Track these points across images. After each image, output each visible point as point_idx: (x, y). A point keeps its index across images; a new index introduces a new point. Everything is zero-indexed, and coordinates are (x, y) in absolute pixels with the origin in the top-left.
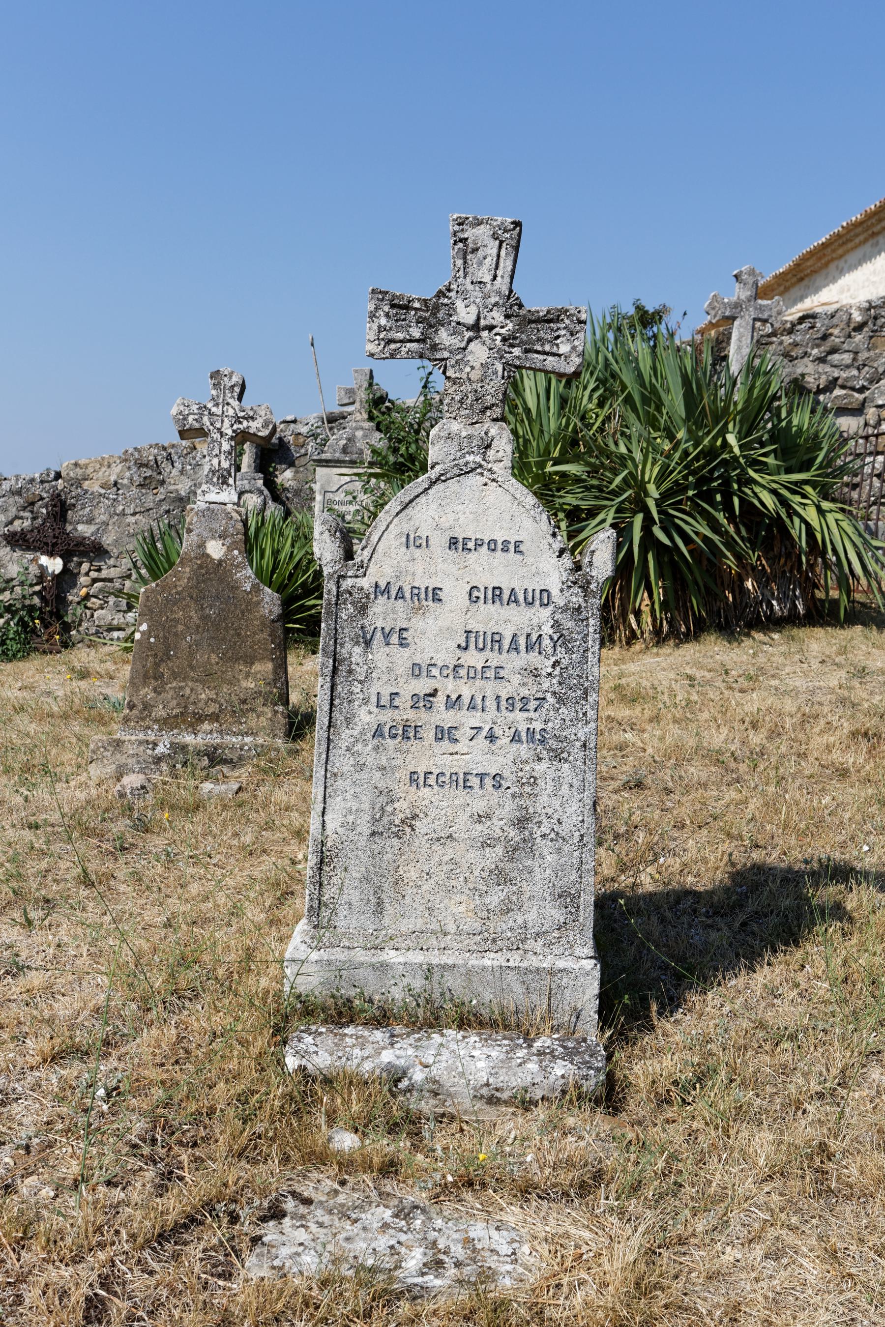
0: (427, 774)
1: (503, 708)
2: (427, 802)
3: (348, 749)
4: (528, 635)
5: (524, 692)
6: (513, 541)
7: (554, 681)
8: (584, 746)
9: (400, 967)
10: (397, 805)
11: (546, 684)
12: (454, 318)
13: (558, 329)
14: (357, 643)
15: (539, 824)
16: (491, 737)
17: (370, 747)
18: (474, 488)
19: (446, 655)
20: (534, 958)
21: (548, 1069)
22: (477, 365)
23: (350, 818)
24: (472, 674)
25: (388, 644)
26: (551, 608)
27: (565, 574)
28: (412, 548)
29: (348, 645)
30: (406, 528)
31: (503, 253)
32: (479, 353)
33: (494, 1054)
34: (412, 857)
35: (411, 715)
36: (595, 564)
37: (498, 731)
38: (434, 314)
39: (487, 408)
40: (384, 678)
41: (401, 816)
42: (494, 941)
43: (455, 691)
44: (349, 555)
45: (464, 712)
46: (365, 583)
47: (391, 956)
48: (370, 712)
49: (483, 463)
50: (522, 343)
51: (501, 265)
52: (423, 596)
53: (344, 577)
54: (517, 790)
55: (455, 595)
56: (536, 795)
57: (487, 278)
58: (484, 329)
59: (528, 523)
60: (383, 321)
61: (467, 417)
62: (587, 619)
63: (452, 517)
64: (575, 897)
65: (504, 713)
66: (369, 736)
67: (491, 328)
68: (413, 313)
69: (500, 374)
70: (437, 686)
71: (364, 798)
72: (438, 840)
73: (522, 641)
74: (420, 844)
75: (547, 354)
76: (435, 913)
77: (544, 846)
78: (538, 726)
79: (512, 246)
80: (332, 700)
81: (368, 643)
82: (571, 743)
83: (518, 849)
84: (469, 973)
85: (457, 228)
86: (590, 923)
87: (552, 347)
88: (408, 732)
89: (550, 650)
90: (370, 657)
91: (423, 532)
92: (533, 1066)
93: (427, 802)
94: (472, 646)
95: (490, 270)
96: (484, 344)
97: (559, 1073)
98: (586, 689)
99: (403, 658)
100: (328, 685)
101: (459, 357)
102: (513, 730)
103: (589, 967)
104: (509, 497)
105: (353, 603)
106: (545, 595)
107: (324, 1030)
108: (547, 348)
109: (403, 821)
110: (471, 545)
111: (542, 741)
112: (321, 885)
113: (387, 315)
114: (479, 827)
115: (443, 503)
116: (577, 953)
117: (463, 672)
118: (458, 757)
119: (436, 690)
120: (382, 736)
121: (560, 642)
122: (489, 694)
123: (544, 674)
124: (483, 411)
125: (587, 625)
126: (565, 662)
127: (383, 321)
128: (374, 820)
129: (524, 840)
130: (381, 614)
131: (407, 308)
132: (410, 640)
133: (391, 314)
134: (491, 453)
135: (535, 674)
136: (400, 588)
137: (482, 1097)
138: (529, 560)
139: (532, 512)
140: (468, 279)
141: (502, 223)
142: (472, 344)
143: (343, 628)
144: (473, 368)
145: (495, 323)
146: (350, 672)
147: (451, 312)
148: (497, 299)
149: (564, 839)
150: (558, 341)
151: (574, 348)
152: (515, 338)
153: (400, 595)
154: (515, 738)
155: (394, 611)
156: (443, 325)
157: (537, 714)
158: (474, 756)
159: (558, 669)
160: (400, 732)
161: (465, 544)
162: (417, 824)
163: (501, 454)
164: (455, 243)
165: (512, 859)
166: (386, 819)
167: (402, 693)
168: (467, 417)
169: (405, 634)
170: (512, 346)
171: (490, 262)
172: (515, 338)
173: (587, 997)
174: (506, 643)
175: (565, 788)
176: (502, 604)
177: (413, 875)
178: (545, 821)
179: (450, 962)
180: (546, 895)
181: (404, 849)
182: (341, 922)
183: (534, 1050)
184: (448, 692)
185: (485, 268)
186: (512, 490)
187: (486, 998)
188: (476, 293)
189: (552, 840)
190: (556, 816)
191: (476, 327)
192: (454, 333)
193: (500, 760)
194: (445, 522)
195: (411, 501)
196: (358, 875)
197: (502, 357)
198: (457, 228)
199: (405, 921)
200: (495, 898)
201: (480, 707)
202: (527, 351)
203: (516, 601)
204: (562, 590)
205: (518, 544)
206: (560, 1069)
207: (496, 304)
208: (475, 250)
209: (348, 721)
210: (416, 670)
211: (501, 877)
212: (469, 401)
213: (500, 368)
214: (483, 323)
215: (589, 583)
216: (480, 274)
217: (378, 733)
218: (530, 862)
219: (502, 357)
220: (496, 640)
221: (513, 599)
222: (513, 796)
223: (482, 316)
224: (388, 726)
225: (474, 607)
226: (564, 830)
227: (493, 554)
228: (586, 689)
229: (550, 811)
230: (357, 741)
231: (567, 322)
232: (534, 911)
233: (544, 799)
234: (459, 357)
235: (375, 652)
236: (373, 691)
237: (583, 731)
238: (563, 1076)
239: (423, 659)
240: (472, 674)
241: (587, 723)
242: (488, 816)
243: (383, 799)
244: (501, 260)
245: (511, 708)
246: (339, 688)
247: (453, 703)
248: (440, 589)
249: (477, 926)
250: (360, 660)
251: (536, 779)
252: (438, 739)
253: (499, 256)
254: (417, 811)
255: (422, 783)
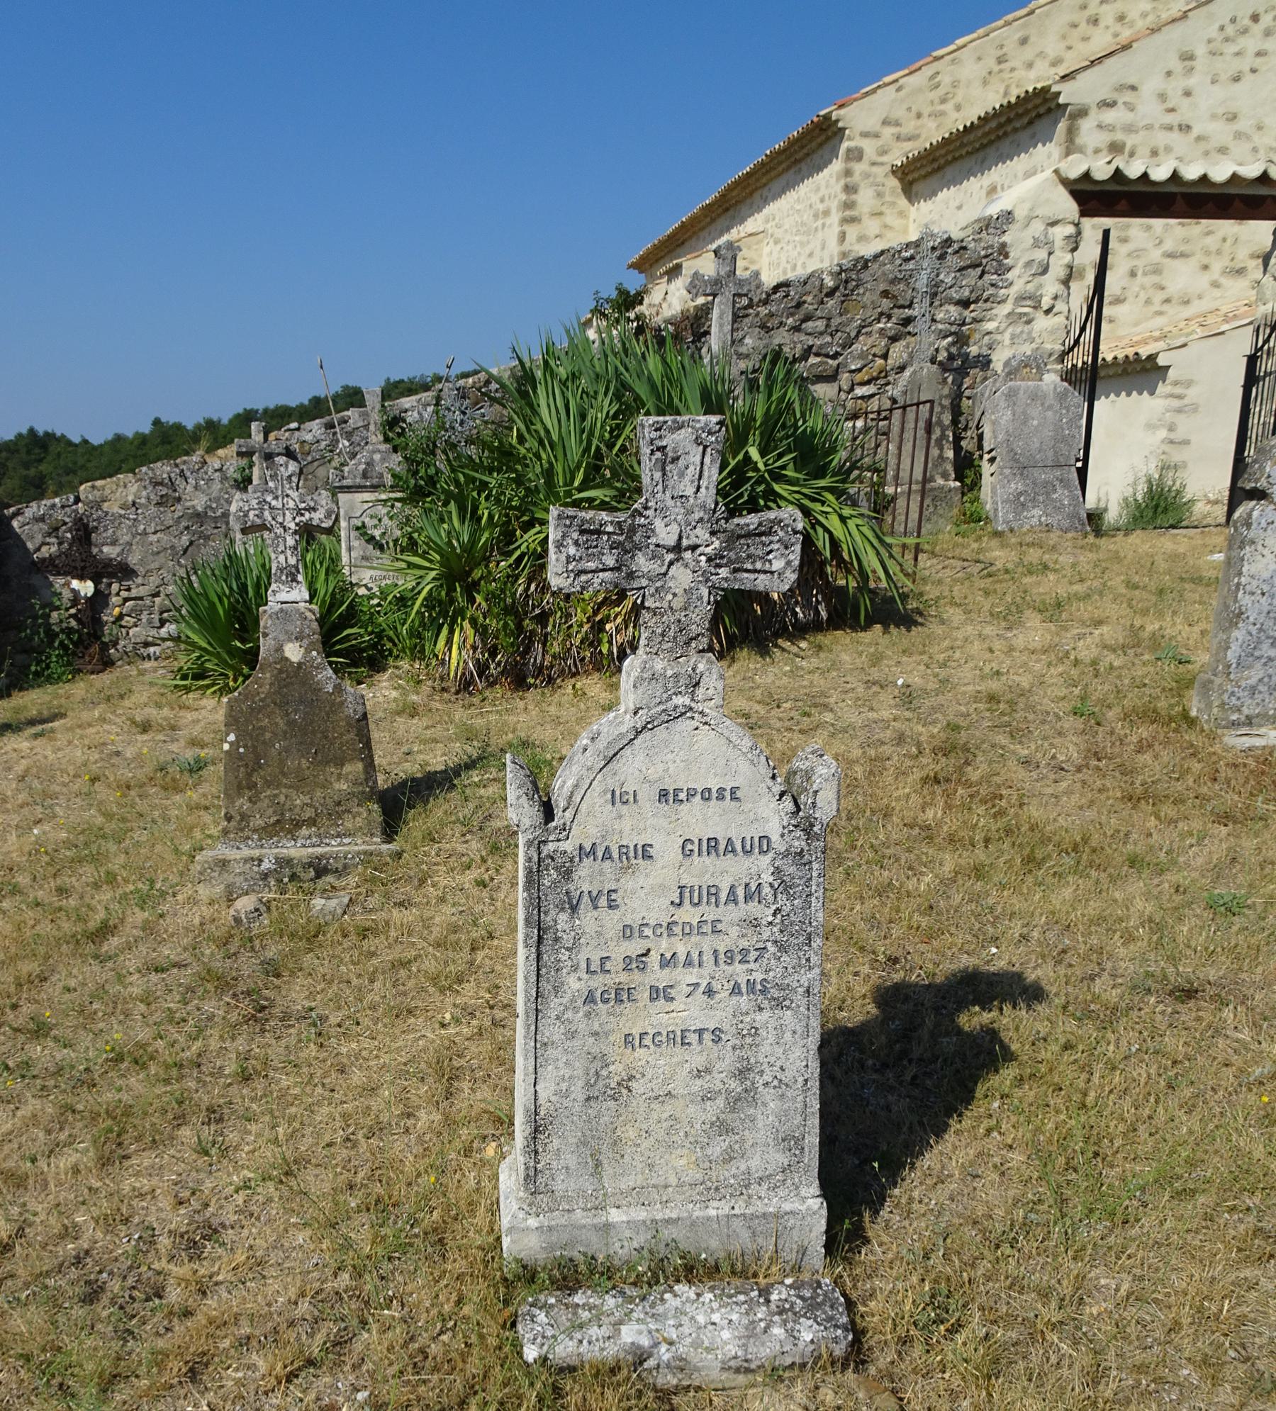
0: (642, 1035)
1: (721, 962)
2: (643, 1063)
3: (558, 1018)
4: (747, 885)
5: (744, 943)
6: (728, 789)
7: (775, 929)
8: (808, 991)
9: (625, 1225)
10: (612, 1068)
11: (766, 933)
12: (653, 540)
13: (771, 542)
14: (563, 909)
15: (761, 1073)
16: (710, 992)
17: (581, 1014)
18: (685, 734)
19: (658, 912)
20: (759, 1203)
21: (795, 1333)
22: (679, 591)
23: (564, 1086)
24: (687, 930)
25: (596, 908)
26: (771, 854)
27: (786, 819)
28: (618, 804)
29: (553, 913)
30: (612, 783)
31: (707, 460)
32: (681, 577)
33: (735, 1317)
34: (630, 1117)
35: (623, 977)
36: (819, 805)
37: (716, 986)
38: (630, 538)
39: (692, 639)
40: (593, 943)
41: (617, 1078)
42: (717, 1189)
43: (669, 949)
44: (548, 811)
45: (680, 969)
46: (568, 846)
47: (615, 1216)
48: (579, 979)
49: (693, 705)
50: (730, 562)
51: (706, 474)
52: (632, 854)
53: (545, 842)
54: (737, 1042)
55: (667, 850)
56: (757, 1046)
57: (690, 491)
58: (687, 549)
59: (744, 767)
60: (572, 550)
61: (670, 651)
62: (810, 862)
63: (660, 767)
64: (799, 1140)
65: (723, 966)
66: (580, 1002)
67: (694, 548)
68: (605, 537)
69: (705, 599)
70: (650, 945)
71: (577, 1064)
72: (656, 1098)
73: (740, 892)
74: (638, 1104)
75: (755, 571)
76: (656, 1168)
77: (767, 1095)
78: (758, 976)
79: (718, 451)
80: (538, 970)
81: (574, 909)
82: (794, 990)
83: (739, 1099)
84: (693, 1224)
85: (654, 434)
86: (816, 1163)
87: (764, 564)
88: (622, 995)
89: (770, 898)
90: (577, 922)
91: (629, 787)
92: (777, 1331)
93: (643, 1063)
94: (687, 901)
95: (692, 482)
96: (686, 566)
97: (808, 1339)
98: (810, 934)
99: (612, 921)
100: (534, 956)
101: (658, 584)
102: (732, 983)
103: (816, 1207)
104: (723, 741)
105: (556, 869)
106: (765, 842)
107: (552, 1300)
108: (759, 565)
109: (619, 1084)
110: (682, 796)
111: (764, 991)
112: (536, 1152)
113: (576, 543)
114: (698, 1082)
115: (651, 753)
116: (803, 1193)
117: (677, 929)
118: (674, 1014)
119: (649, 950)
120: (593, 1001)
121: (781, 889)
122: (707, 949)
123: (764, 922)
124: (687, 644)
125: (811, 869)
126: (786, 909)
127: (572, 550)
128: (589, 1086)
129: (746, 1090)
130: (586, 878)
131: (598, 532)
132: (619, 901)
133: (581, 542)
134: (700, 692)
135: (755, 924)
136: (607, 848)
137: (730, 1368)
138: (747, 806)
139: (749, 755)
140: (668, 494)
141: (706, 425)
142: (674, 568)
143: (546, 895)
144: (675, 595)
145: (699, 542)
146: (557, 940)
147: (649, 533)
148: (701, 514)
149: (787, 1085)
150: (771, 557)
151: (789, 563)
152: (722, 557)
153: (607, 855)
154: (736, 991)
155: (601, 873)
156: (640, 550)
157: (757, 965)
158: (688, 1013)
159: (779, 916)
160: (613, 996)
161: (676, 795)
162: (634, 1085)
163: (711, 692)
164: (652, 452)
165: (733, 1110)
166: (601, 1083)
167: (613, 956)
168: (670, 651)
169: (613, 896)
170: (719, 566)
171: (692, 472)
172: (722, 557)
173: (813, 1234)
174: (723, 896)
175: (788, 1035)
176: (718, 855)
177: (632, 1134)
178: (767, 1070)
179: (674, 1216)
180: (770, 1140)
181: (622, 1110)
182: (559, 1187)
183: (773, 1307)
184: (662, 951)
185: (687, 479)
186: (726, 733)
187: (711, 1247)
188: (677, 511)
189: (775, 1087)
190: (778, 1064)
191: (677, 548)
192: (653, 558)
193: (720, 1014)
194: (653, 773)
195: (615, 755)
196: (575, 1140)
197: (707, 580)
198: (654, 434)
199: (625, 1179)
200: (718, 1148)
201: (697, 963)
202: (735, 571)
203: (733, 851)
204: (782, 835)
205: (734, 790)
206: (807, 1332)
207: (701, 520)
208: (675, 459)
209: (556, 990)
210: (627, 932)
211: (722, 1127)
212: (672, 633)
213: (705, 592)
214: (685, 543)
215: (812, 825)
216: (682, 487)
217: (590, 999)
218: (752, 1111)
219: (707, 580)
220: (713, 893)
221: (730, 848)
222: (734, 1048)
223: (684, 535)
224: (599, 992)
225: (688, 860)
226: (787, 1077)
227: (708, 803)
228: (810, 934)
229: (772, 1059)
230: (567, 1008)
231: (781, 533)
232: (757, 1157)
233: (765, 1048)
234: (658, 584)
235: (582, 917)
236: (582, 957)
237: (806, 977)
238: (812, 1341)
239: (633, 919)
240: (687, 930)
241: (810, 968)
242: (708, 1071)
243: (597, 1064)
244: (705, 468)
245: (730, 959)
246: (545, 957)
247: (667, 962)
248: (651, 846)
249: (699, 1176)
250: (566, 927)
251: (757, 1029)
252: (652, 999)
253: (702, 463)
254: (634, 1073)
255: (637, 1044)
